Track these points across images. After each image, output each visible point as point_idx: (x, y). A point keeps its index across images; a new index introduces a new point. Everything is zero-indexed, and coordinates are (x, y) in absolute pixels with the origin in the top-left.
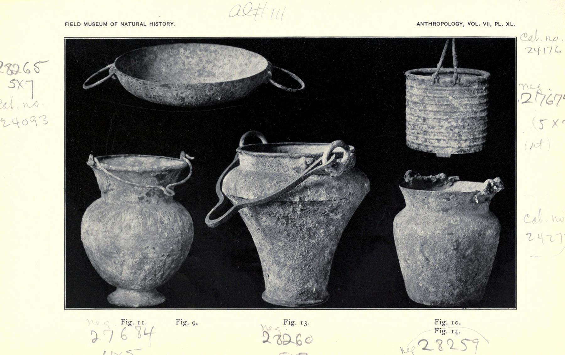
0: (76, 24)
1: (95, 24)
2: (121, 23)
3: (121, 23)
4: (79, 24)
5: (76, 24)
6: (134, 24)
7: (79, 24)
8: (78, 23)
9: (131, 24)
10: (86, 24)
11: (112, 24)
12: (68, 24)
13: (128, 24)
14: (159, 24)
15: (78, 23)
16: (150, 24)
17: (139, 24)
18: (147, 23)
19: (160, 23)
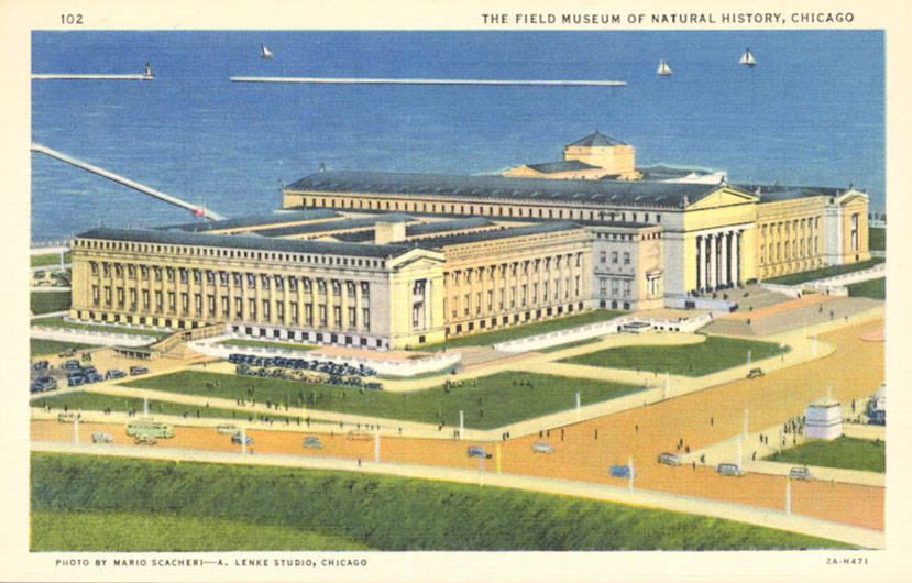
0: (545, 19)
1: (591, 18)
2: (654, 17)
3: (654, 17)
4: (552, 19)
5: (545, 19)
6: (683, 19)
7: (552, 19)
8: (549, 16)
9: (677, 18)
10: (566, 19)
11: (632, 19)
12: (523, 18)
13: (670, 19)
14: (746, 18)
15: (549, 16)
16: (724, 18)
17: (698, 19)
18: (717, 17)
19: (749, 15)
